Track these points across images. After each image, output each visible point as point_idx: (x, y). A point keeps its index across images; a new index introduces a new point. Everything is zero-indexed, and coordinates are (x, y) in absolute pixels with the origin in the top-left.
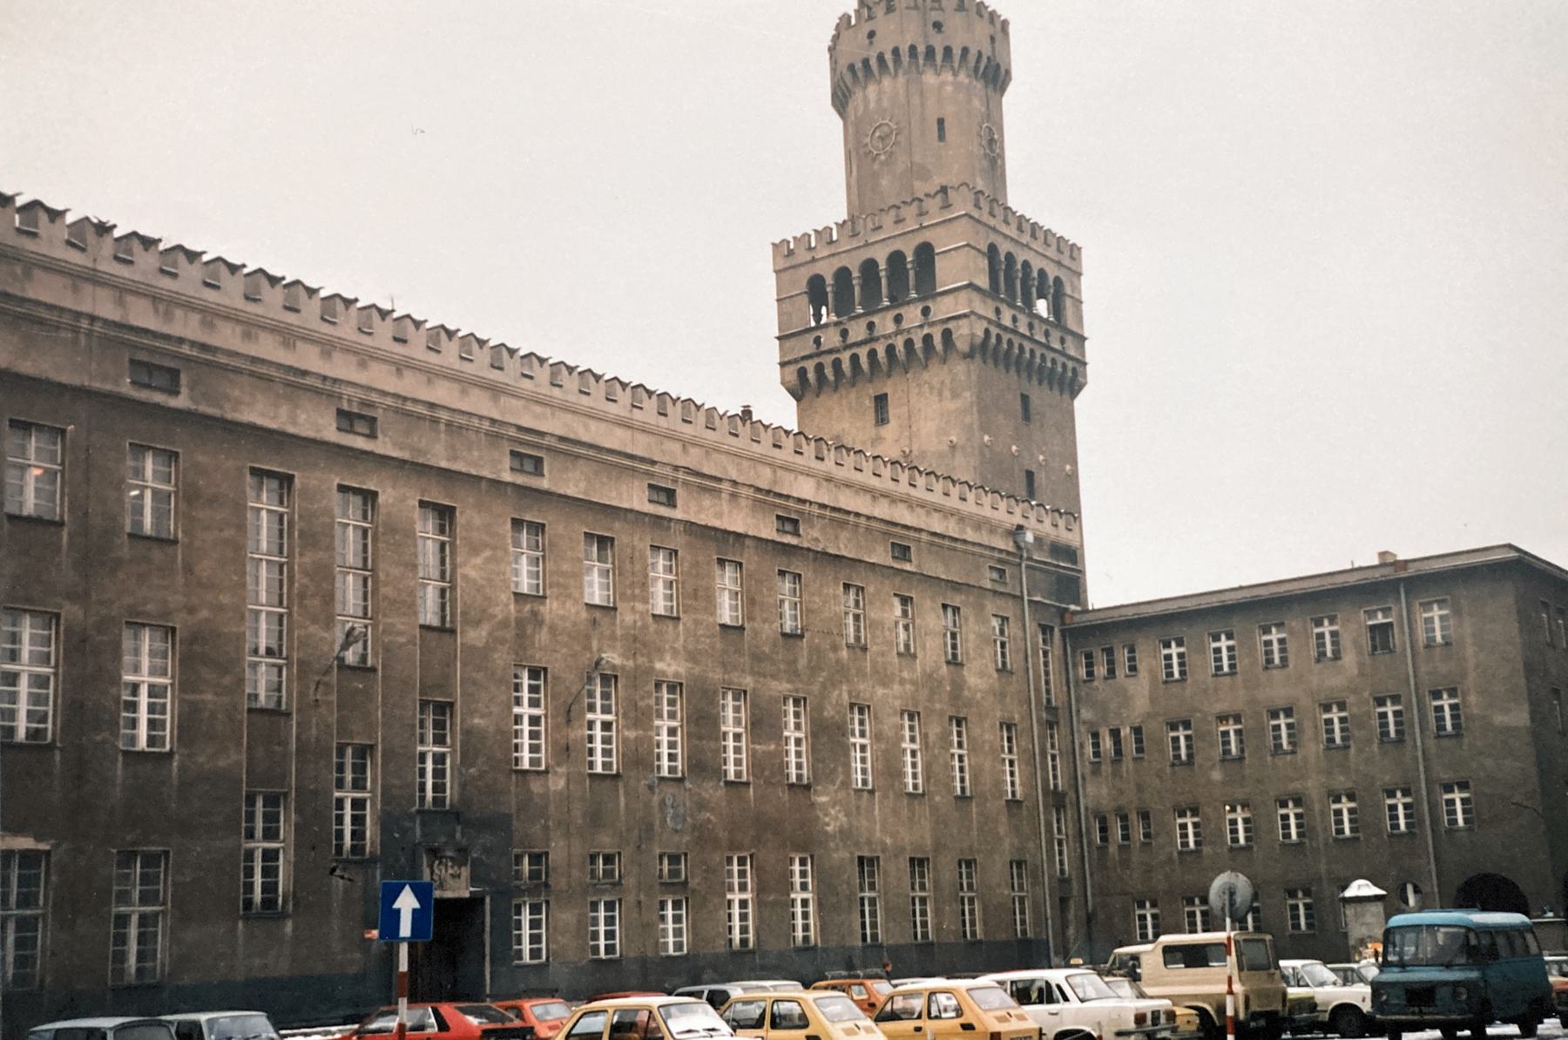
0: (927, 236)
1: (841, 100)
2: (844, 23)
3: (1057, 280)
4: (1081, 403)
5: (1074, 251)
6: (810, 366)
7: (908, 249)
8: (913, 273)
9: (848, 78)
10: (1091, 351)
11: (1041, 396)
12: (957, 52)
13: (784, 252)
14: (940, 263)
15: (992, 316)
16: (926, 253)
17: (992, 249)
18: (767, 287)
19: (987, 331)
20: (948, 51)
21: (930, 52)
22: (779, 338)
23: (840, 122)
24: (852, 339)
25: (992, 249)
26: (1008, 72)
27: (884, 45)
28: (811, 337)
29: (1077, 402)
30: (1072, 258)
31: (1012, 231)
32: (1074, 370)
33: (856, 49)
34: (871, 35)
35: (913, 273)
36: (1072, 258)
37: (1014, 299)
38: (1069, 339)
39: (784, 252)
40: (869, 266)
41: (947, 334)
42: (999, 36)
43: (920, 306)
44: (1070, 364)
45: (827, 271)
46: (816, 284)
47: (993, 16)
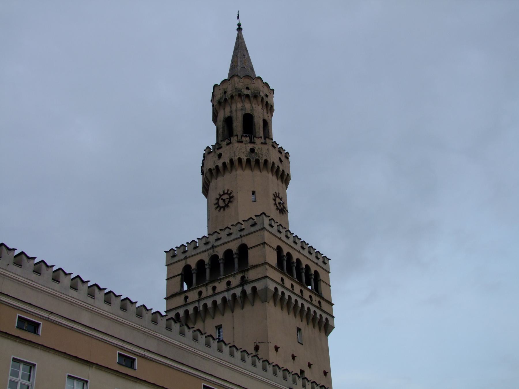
0: (245, 241)
1: (206, 190)
2: (208, 151)
3: (316, 272)
4: (331, 337)
5: (326, 261)
6: (181, 312)
7: (234, 247)
8: (238, 259)
9: (208, 175)
10: (336, 311)
11: (309, 331)
12: (262, 161)
13: (171, 254)
14: (249, 251)
15: (280, 282)
16: (243, 249)
17: (279, 250)
18: (162, 273)
19: (276, 289)
20: (257, 162)
21: (248, 161)
22: (165, 298)
23: (206, 200)
24: (204, 295)
25: (279, 250)
26: (288, 175)
27: (226, 159)
28: (183, 297)
29: (330, 337)
30: (324, 263)
31: (290, 242)
32: (327, 319)
33: (213, 162)
34: (220, 156)
35: (238, 259)
36: (324, 263)
37: (292, 275)
38: (323, 302)
39: (171, 254)
40: (214, 258)
41: (254, 289)
42: (283, 158)
43: (239, 277)
44: (324, 316)
45: (193, 263)
46: (187, 268)
47: (281, 150)
